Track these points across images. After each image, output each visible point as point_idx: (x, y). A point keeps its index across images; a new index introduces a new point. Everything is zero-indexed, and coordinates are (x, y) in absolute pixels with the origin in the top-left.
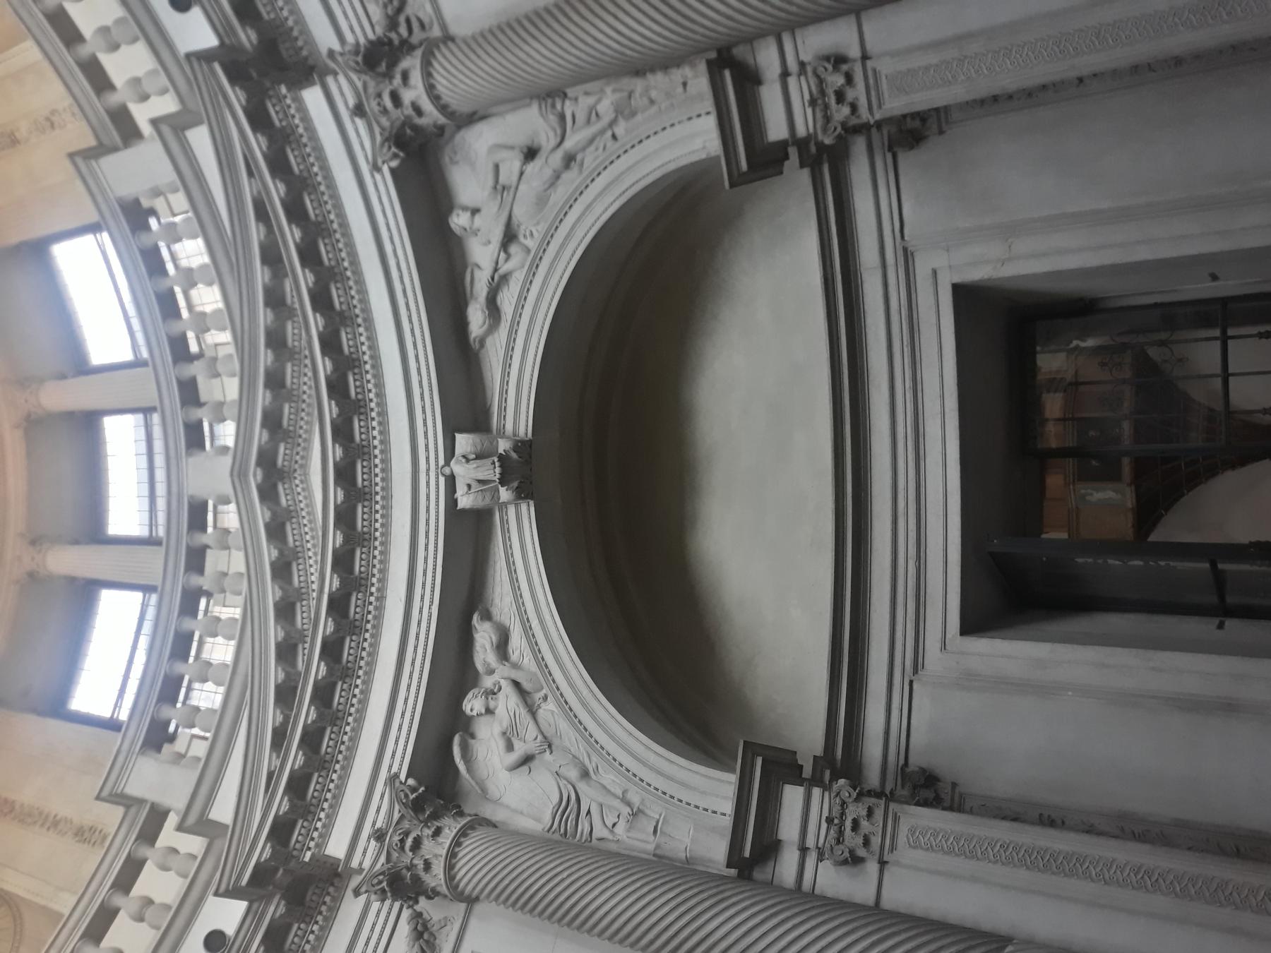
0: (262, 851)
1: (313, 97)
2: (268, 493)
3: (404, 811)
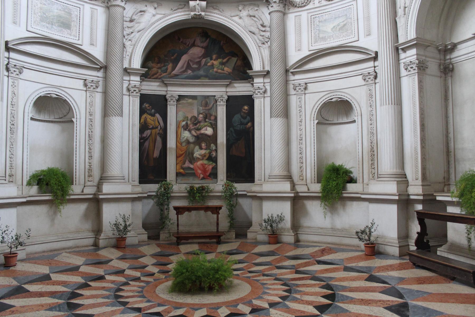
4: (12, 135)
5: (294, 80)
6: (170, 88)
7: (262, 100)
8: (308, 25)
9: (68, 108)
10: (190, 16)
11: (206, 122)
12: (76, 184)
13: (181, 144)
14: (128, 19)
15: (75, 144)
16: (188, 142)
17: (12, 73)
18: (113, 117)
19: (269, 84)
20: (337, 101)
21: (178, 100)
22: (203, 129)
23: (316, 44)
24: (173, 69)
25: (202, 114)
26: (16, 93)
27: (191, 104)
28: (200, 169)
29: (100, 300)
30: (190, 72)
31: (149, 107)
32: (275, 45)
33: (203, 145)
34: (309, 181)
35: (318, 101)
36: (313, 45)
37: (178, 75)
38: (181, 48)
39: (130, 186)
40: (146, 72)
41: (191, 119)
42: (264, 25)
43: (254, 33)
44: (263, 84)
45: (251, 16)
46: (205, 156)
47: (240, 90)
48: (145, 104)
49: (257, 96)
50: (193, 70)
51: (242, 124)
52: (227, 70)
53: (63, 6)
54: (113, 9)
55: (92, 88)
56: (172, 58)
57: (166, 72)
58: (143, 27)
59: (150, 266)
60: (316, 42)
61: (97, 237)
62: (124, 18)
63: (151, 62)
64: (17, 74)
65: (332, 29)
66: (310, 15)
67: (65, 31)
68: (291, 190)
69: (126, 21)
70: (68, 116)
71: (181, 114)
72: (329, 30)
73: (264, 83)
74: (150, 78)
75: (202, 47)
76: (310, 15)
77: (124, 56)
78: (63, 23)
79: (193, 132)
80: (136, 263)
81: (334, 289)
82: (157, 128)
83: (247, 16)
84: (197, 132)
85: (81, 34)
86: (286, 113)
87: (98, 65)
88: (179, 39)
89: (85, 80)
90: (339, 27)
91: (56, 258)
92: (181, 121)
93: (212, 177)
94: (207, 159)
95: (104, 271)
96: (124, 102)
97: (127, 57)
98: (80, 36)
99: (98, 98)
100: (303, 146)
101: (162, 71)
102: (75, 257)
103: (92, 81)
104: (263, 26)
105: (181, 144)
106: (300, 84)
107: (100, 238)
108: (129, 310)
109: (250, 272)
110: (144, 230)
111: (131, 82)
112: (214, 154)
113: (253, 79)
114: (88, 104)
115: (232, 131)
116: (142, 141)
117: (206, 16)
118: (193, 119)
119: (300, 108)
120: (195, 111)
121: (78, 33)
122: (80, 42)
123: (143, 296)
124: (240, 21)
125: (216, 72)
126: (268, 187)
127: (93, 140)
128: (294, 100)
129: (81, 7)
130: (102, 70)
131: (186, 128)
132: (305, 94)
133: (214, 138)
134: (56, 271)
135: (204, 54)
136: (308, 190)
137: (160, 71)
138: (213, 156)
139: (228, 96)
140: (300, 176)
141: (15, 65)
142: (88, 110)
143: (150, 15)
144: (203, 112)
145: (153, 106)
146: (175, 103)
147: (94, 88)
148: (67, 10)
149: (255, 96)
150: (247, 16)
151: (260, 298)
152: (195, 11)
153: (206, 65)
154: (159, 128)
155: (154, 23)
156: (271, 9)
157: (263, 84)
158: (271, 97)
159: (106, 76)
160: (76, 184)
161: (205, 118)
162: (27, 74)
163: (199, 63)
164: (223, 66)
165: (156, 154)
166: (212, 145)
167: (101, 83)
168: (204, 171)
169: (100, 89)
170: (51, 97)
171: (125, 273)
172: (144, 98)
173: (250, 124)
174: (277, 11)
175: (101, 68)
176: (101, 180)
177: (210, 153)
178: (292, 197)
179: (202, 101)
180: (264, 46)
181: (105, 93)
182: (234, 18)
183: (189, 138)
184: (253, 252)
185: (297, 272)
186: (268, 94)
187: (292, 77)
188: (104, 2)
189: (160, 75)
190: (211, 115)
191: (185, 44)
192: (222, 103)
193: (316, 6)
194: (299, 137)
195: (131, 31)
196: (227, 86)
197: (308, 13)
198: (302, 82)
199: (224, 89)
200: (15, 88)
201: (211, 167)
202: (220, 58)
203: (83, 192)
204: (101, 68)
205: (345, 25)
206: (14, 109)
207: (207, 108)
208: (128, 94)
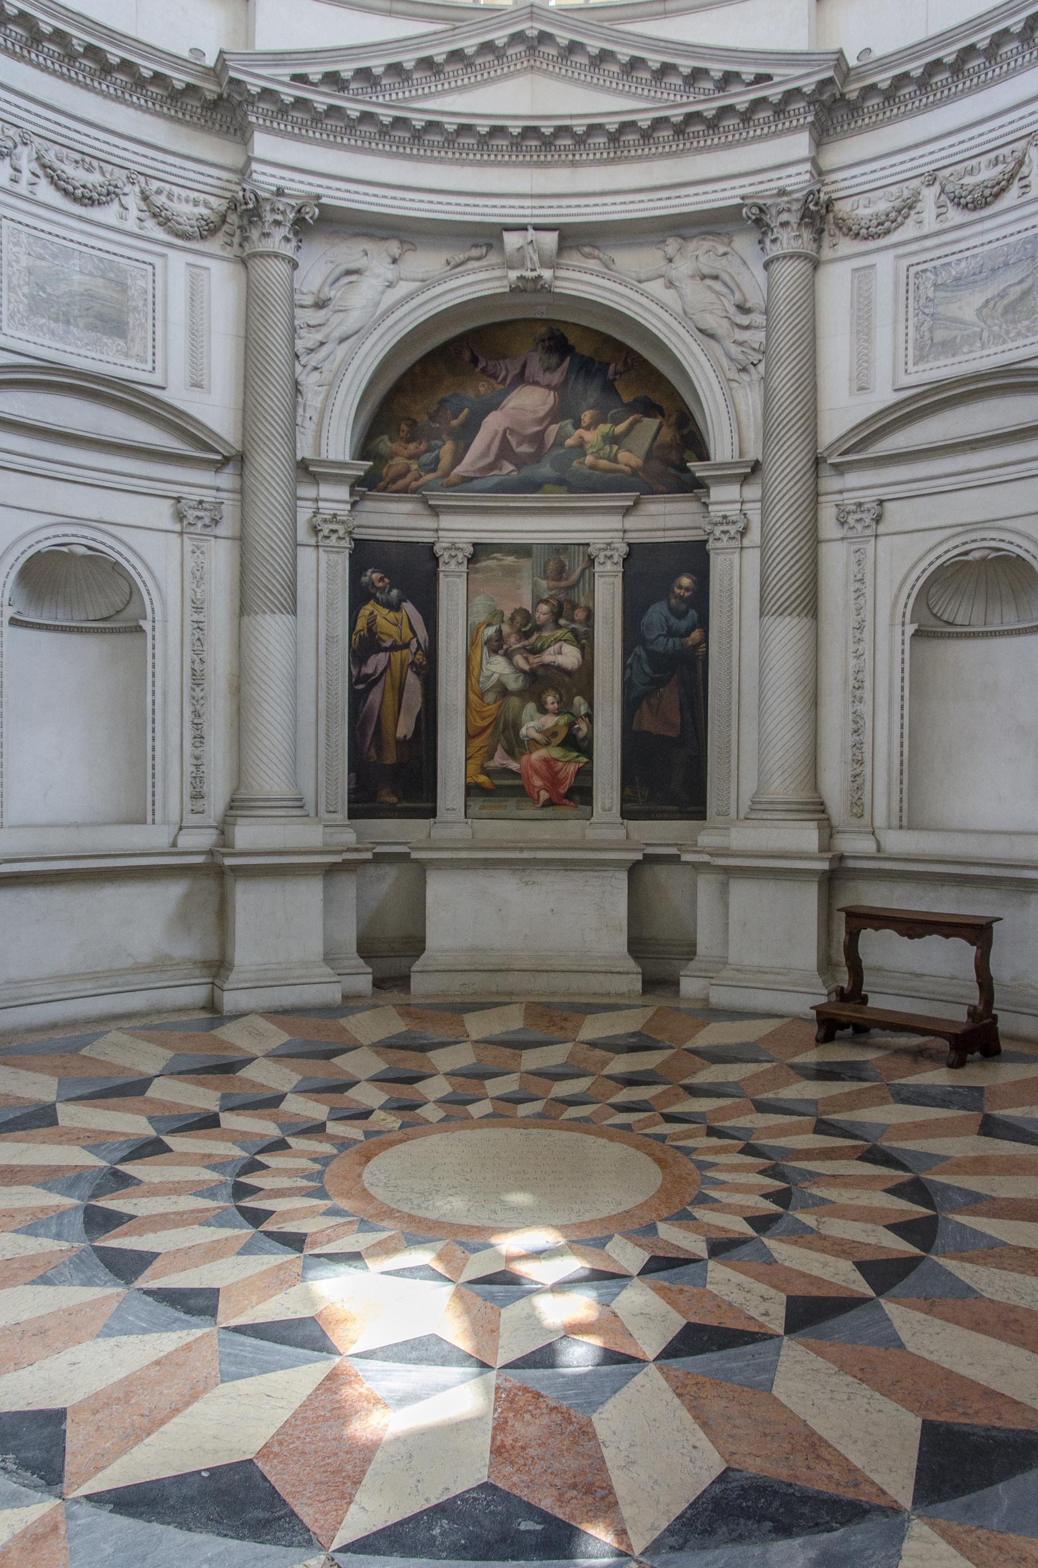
0: (254, 86)
1: (800, 145)
2: (517, 38)
3: (297, 208)
5: (841, 492)
6: (446, 521)
7: (737, 555)
8: (896, 300)
9: (128, 591)
10: (505, 283)
11: (559, 627)
12: (154, 822)
13: (482, 696)
14: (309, 300)
15: (149, 698)
16: (503, 691)
18: (267, 617)
19: (758, 505)
20: (984, 559)
21: (472, 560)
22: (551, 649)
23: (921, 367)
24: (457, 460)
25: (546, 601)
27: (511, 572)
28: (537, 772)
29: (188, 1203)
30: (511, 467)
31: (381, 579)
32: (784, 376)
33: (550, 700)
34: (880, 820)
35: (920, 559)
36: (911, 368)
37: (471, 479)
38: (482, 389)
39: (321, 827)
40: (370, 472)
41: (512, 619)
42: (748, 305)
43: (712, 336)
44: (738, 506)
45: (704, 277)
46: (555, 734)
47: (669, 525)
48: (369, 573)
49: (718, 544)
50: (520, 462)
51: (671, 633)
52: (629, 458)
53: (101, 259)
54: (259, 266)
55: (200, 524)
56: (454, 423)
57: (434, 470)
58: (357, 326)
59: (363, 1084)
60: (920, 358)
61: (217, 982)
62: (296, 297)
63: (386, 438)
65: (979, 311)
66: (905, 263)
67: (109, 342)
68: (820, 851)
69: (302, 306)
70: (131, 611)
71: (481, 603)
72: (969, 314)
73: (742, 503)
74: (384, 489)
75: (548, 387)
76: (905, 263)
77: (299, 420)
78: (100, 317)
79: (519, 660)
80: (319, 1071)
81: (937, 1199)
82: (407, 646)
83: (692, 277)
84: (531, 658)
85: (159, 351)
86: (810, 604)
87: (217, 452)
88: (475, 361)
89: (178, 500)
90: (1006, 301)
91: (84, 1052)
92: (480, 625)
93: (577, 798)
94: (562, 745)
95: (224, 1097)
96: (299, 569)
97: (308, 424)
98: (159, 358)
99: (220, 557)
100: (866, 709)
101: (420, 466)
102: (144, 1046)
103: (201, 502)
104: (743, 309)
105: (482, 696)
106: (860, 505)
107: (226, 986)
108: (269, 1243)
109: (669, 1118)
110: (361, 961)
111: (321, 504)
112: (583, 727)
113: (707, 488)
114: (188, 576)
115: (639, 657)
116: (361, 687)
117: (558, 283)
118: (519, 618)
119: (858, 585)
120: (524, 592)
121: (150, 350)
122: (156, 379)
123: (321, 1193)
124: (669, 296)
125: (593, 467)
126: (748, 838)
127: (205, 686)
128: (836, 559)
129: (158, 262)
130: (229, 469)
131: (497, 644)
132: (876, 536)
133: (581, 681)
134: (79, 1092)
135: (552, 408)
136: (879, 850)
137: (414, 466)
138: (581, 735)
139: (629, 544)
140: (854, 804)
142: (189, 594)
143: (378, 283)
144: (552, 597)
145: (392, 576)
146: (464, 568)
147: (206, 526)
148: (112, 275)
149: (710, 545)
150: (692, 277)
151: (682, 1217)
152: (522, 265)
153: (562, 445)
154: (414, 645)
155: (390, 311)
156: (773, 251)
157: (738, 506)
158: (763, 547)
159: (242, 487)
160: (154, 822)
161: (557, 613)
163: (538, 439)
164: (615, 447)
165: (405, 728)
166: (578, 700)
167: (229, 510)
168: (553, 780)
169: (225, 529)
170: (72, 555)
171: (283, 1106)
172: (364, 554)
173: (696, 635)
174: (791, 256)
175: (226, 460)
176: (231, 808)
177: (571, 725)
178: (824, 872)
179: (546, 564)
180: (745, 377)
181: (242, 539)
182: (647, 286)
183: (504, 679)
184: (689, 1045)
185: (823, 1127)
186: (754, 536)
187: (830, 483)
188: (231, 245)
189: (416, 480)
190: (575, 606)
191: (495, 376)
192: (609, 567)
193: (926, 231)
194: (851, 677)
195: (319, 336)
196: (627, 511)
197: (899, 257)
198: (869, 497)
199: (615, 522)
201: (572, 768)
202: (605, 422)
203: (174, 844)
204: (226, 460)
205: (1026, 293)
207: (563, 584)
208: (313, 542)
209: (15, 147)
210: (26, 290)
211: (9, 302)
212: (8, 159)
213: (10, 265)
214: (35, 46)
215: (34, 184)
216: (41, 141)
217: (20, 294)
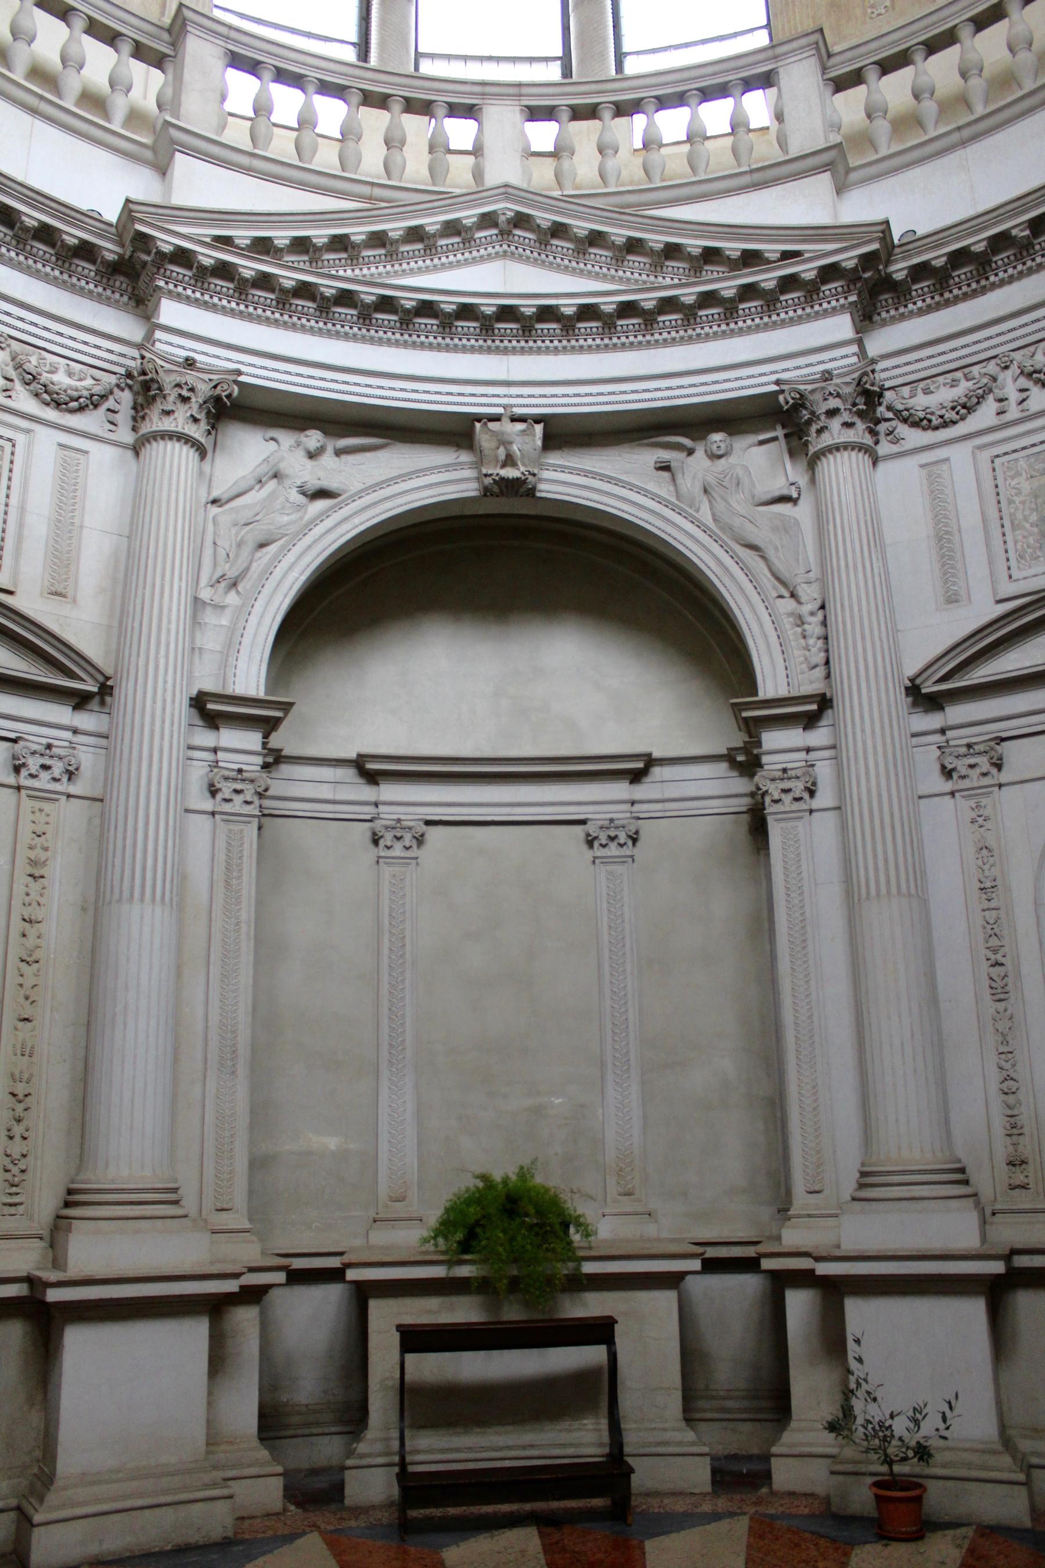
4: (1001, 1006)
17: (963, 777)
26: (992, 843)
64: (984, 775)
141: (969, 746)
162: (1020, 757)
200: (988, 825)
206: (993, 904)
209: (994, 379)
210: (1034, 517)
211: (1016, 542)
212: (991, 397)
213: (1010, 502)
214: (988, 268)
215: (1023, 400)
216: (1021, 352)
217: (1027, 525)
